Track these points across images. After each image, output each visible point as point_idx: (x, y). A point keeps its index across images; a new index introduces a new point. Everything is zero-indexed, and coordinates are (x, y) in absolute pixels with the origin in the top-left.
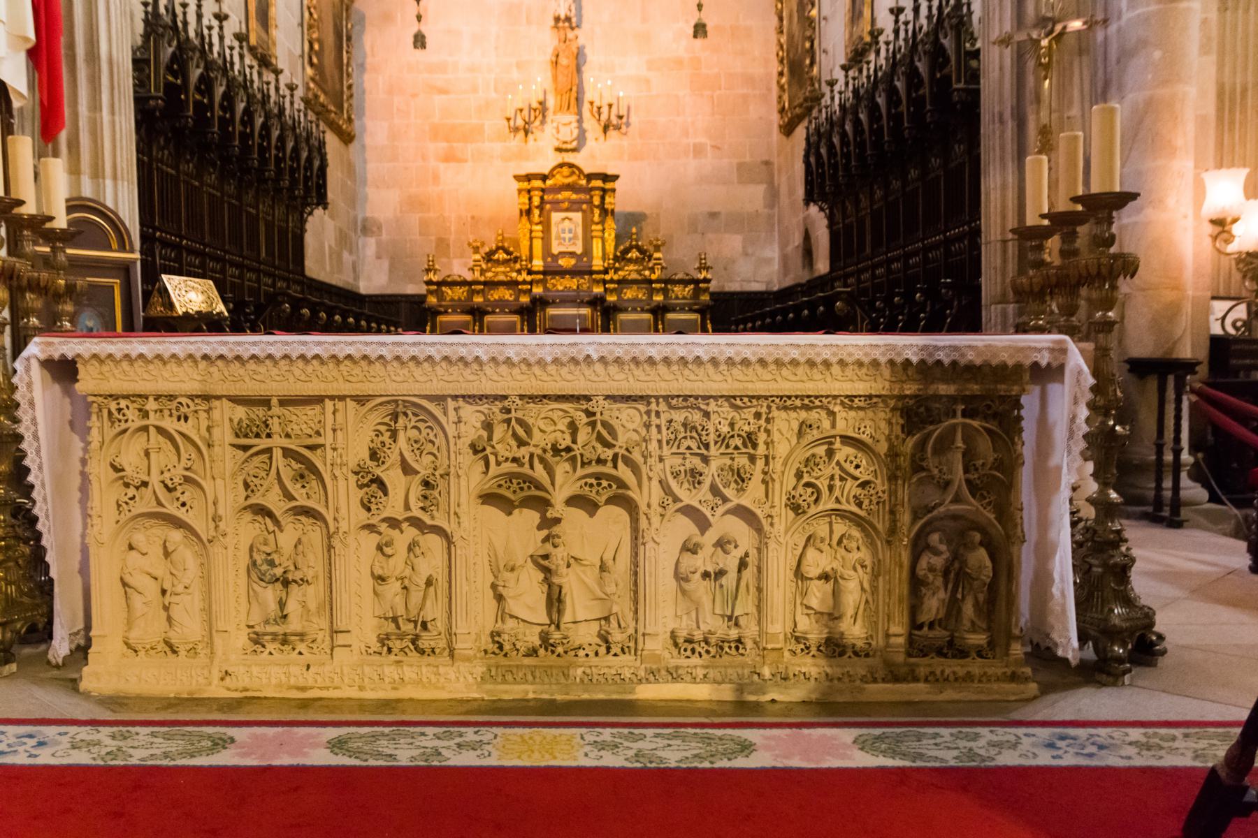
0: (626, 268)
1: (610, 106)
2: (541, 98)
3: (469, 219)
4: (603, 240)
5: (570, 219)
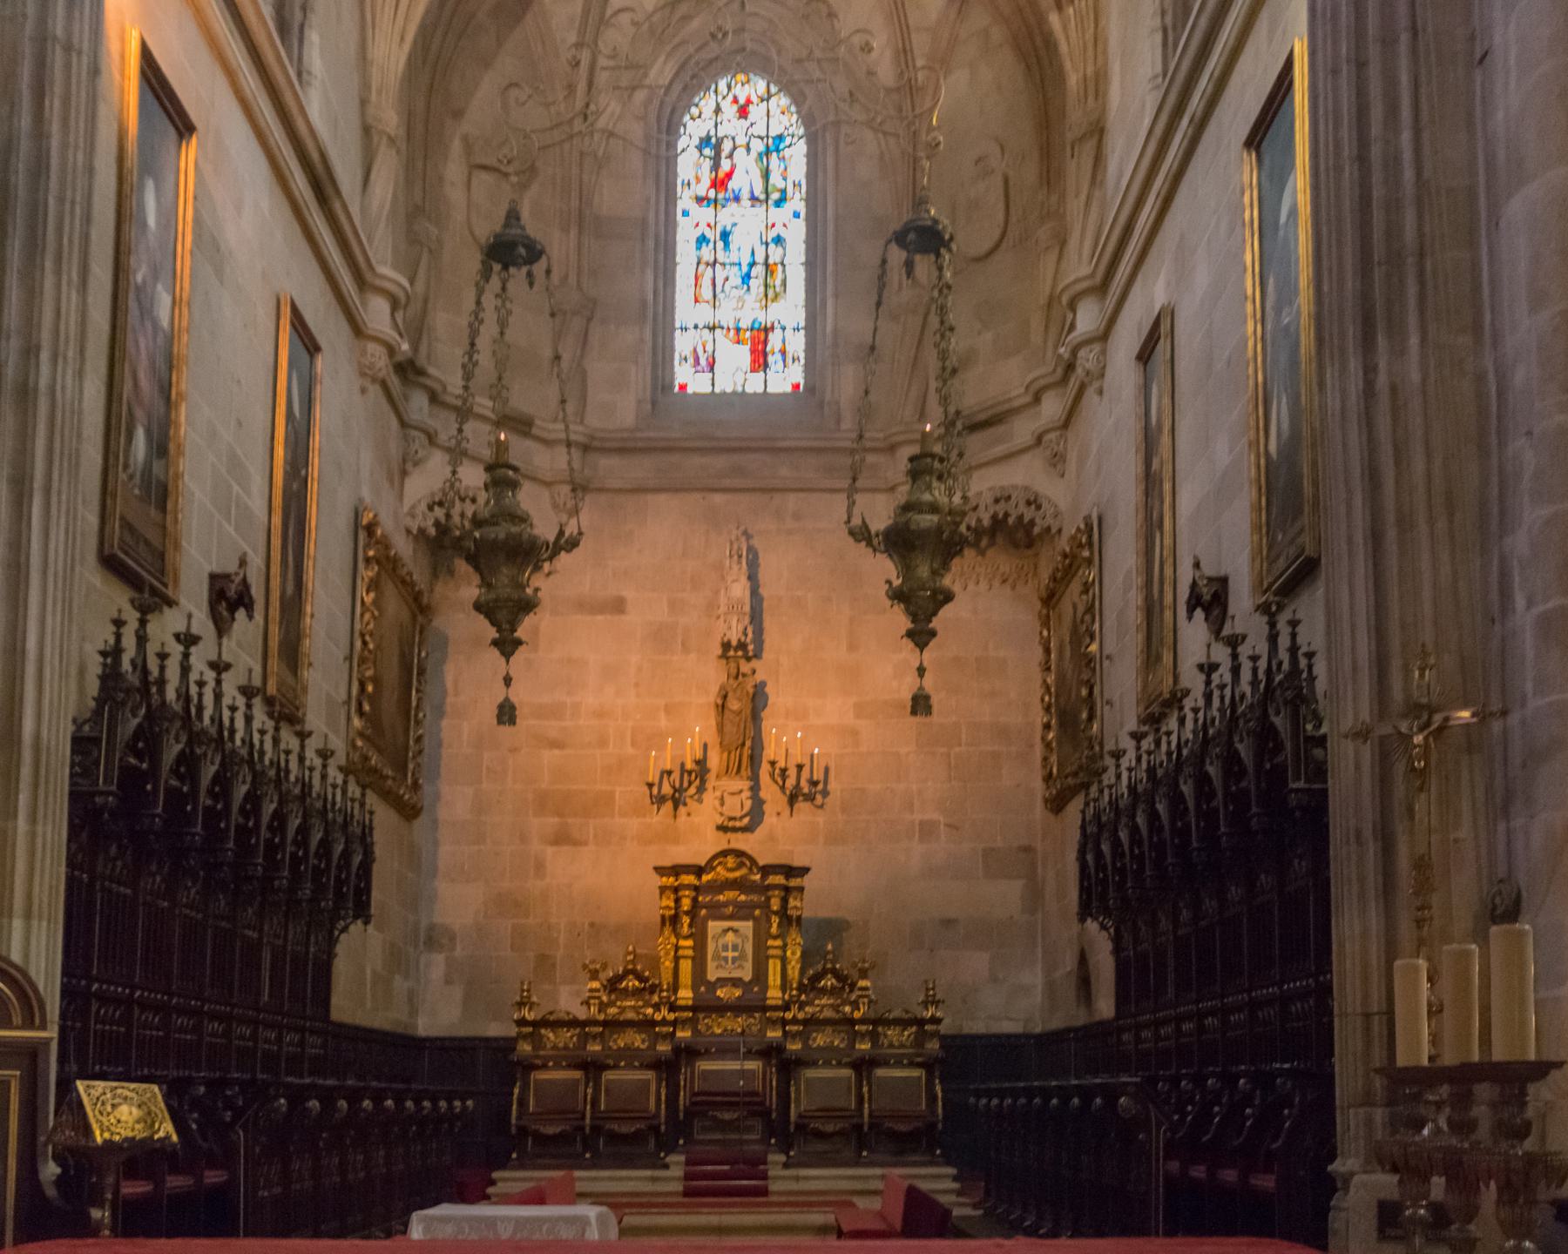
0: (817, 1002)
1: (800, 767)
2: (699, 755)
3: (586, 926)
4: (784, 960)
5: (735, 931)
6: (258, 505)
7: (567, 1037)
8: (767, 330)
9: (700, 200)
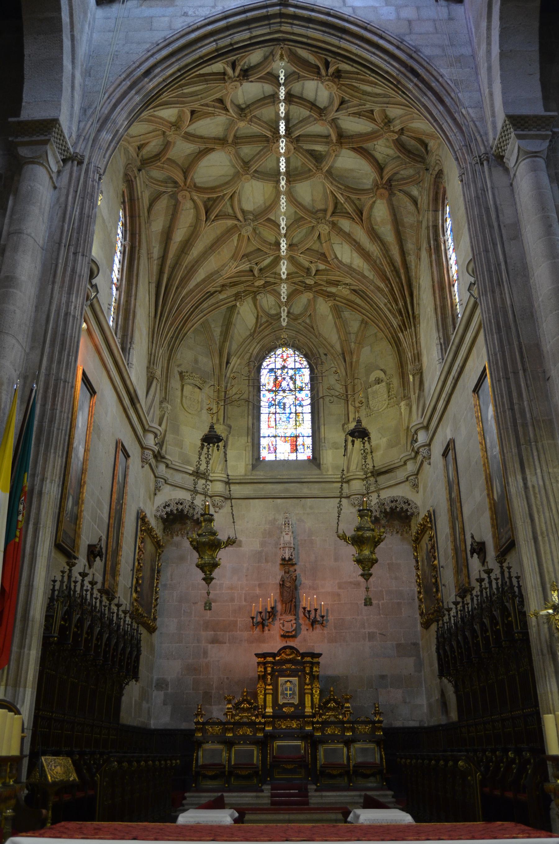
1: (316, 610)
4: (312, 695)
5: (290, 682)
6: (105, 516)
7: (217, 729)
8: (297, 437)
9: (269, 391)
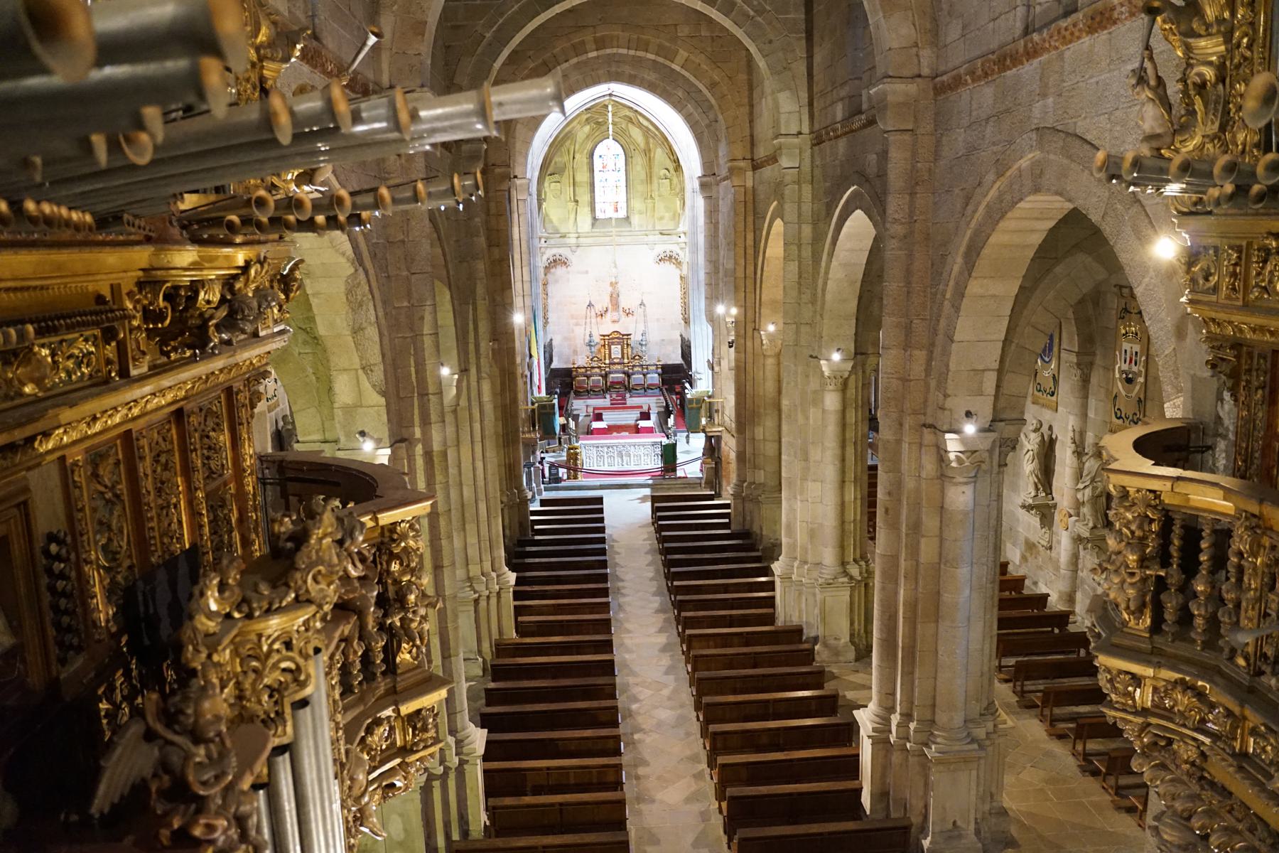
7: (583, 370)
